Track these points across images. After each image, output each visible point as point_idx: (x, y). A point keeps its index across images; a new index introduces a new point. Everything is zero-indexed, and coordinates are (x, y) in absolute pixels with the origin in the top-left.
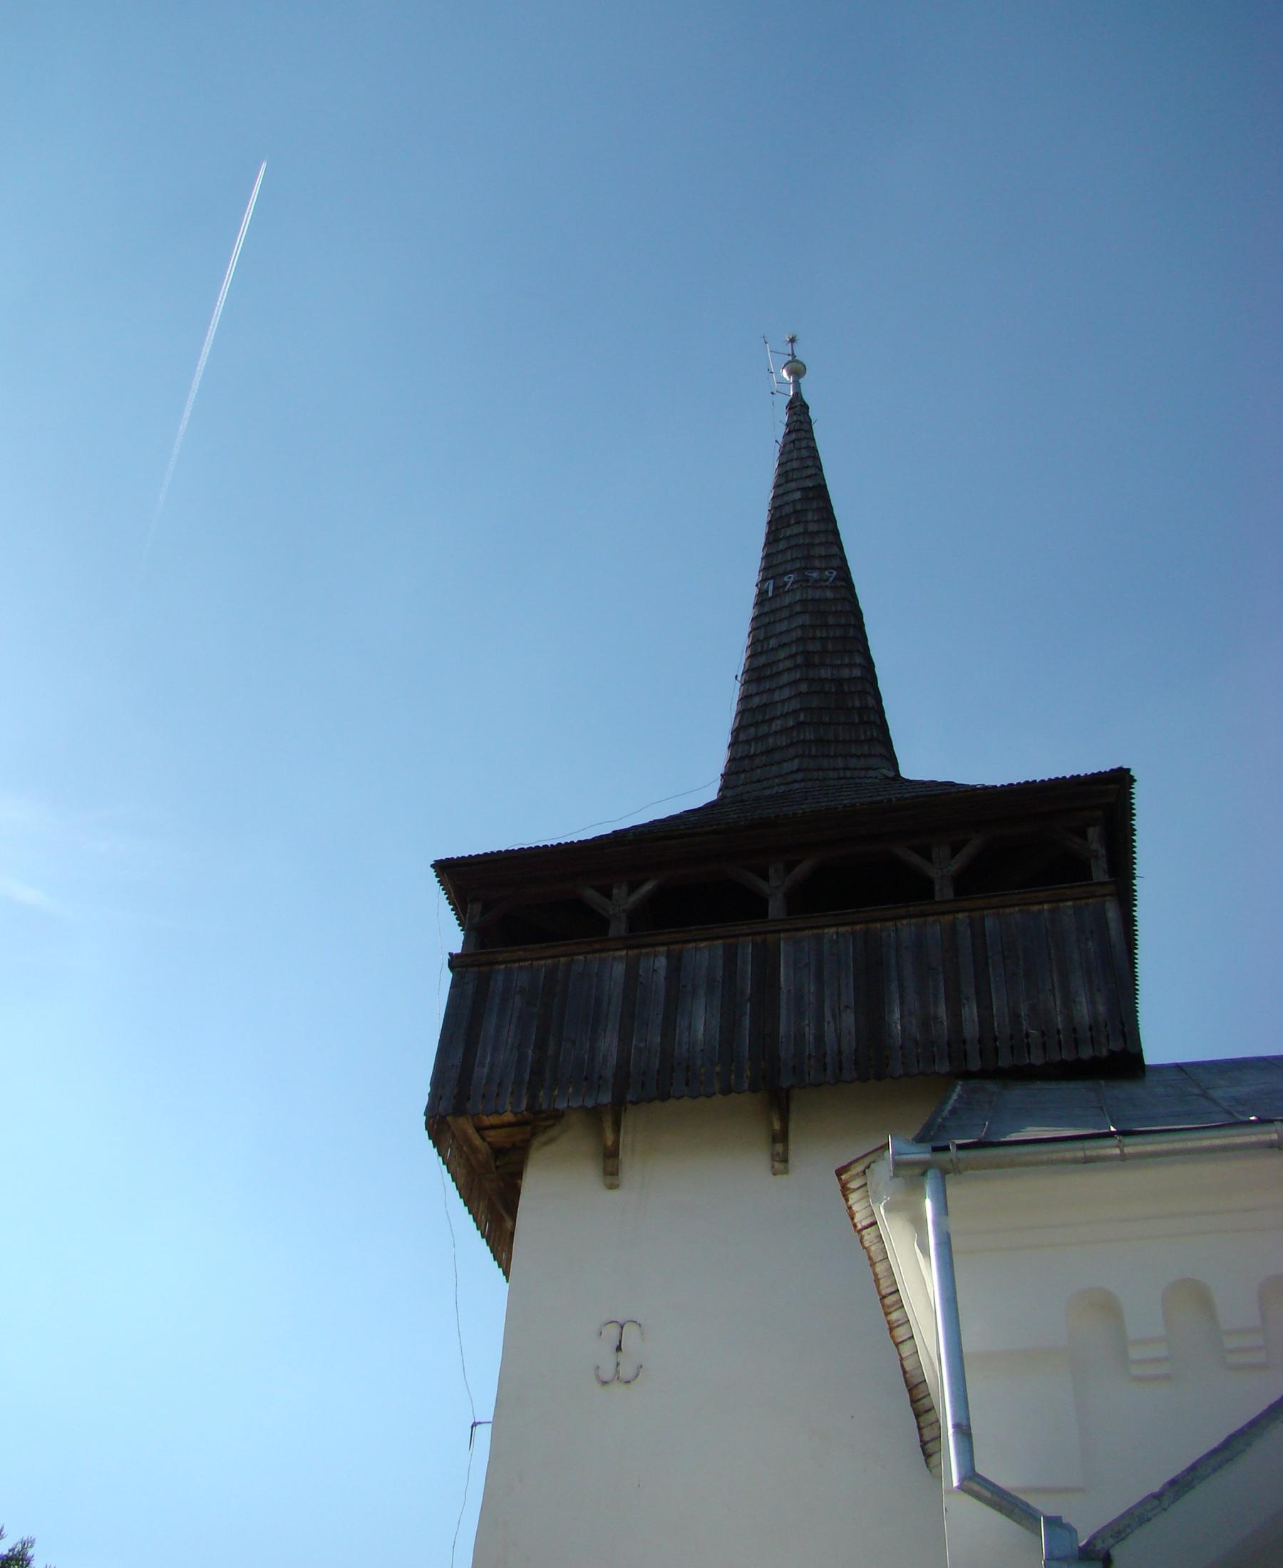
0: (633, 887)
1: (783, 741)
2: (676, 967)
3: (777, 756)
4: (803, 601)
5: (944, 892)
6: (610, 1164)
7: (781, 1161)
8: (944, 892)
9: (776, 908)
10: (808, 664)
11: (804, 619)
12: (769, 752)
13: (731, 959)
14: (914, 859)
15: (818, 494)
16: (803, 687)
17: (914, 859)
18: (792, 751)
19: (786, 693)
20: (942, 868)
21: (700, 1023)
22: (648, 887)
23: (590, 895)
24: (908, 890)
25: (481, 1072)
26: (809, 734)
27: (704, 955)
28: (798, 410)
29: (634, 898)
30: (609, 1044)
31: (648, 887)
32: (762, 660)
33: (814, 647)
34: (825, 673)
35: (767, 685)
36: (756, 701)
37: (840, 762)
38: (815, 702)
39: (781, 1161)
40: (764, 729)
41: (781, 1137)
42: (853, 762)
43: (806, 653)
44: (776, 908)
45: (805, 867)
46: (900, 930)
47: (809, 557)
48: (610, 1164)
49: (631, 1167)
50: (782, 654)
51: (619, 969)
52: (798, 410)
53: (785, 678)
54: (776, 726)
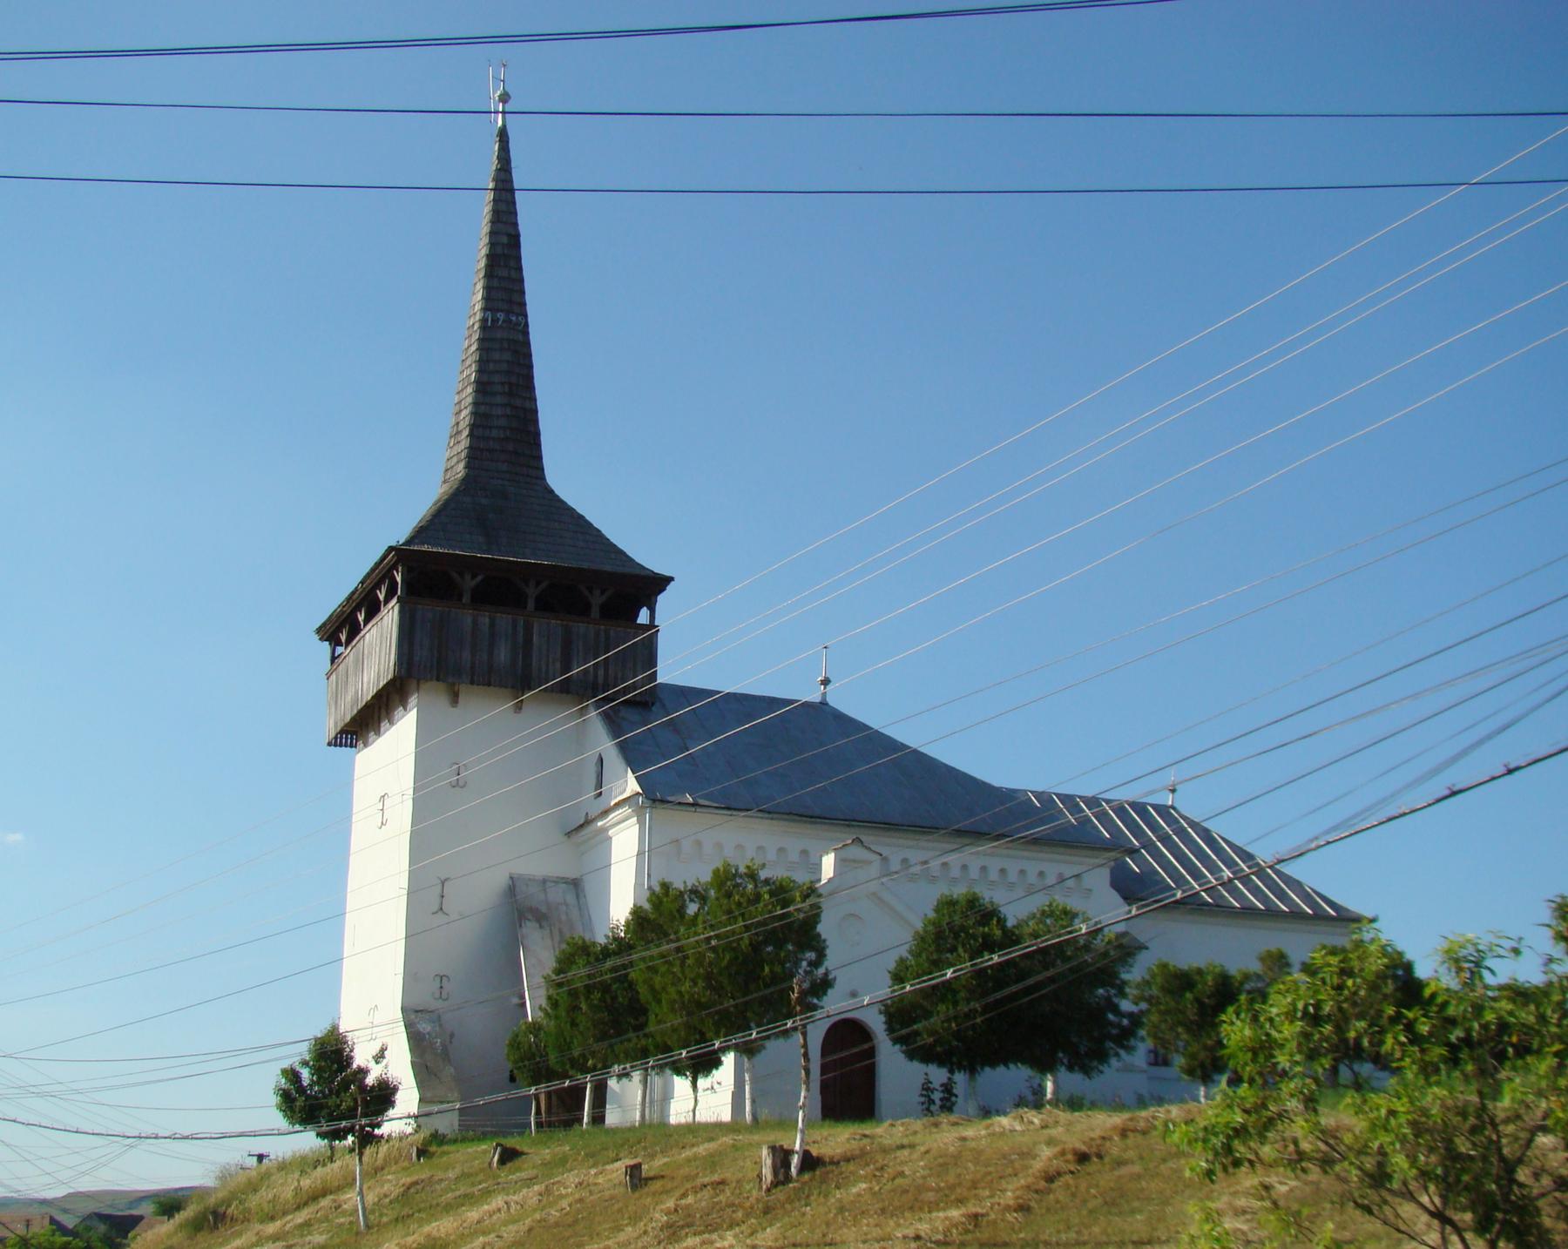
0: (474, 577)
2: (492, 625)
5: (595, 613)
6: (455, 699)
8: (595, 613)
9: (531, 604)
11: (507, 356)
13: (515, 627)
14: (586, 593)
15: (514, 241)
16: (508, 411)
17: (586, 593)
19: (499, 411)
20: (597, 600)
21: (503, 655)
22: (480, 578)
23: (455, 575)
24: (583, 610)
25: (416, 659)
26: (510, 447)
27: (504, 620)
28: (503, 135)
29: (474, 583)
30: (466, 655)
31: (480, 578)
32: (485, 378)
33: (514, 380)
36: (482, 409)
44: (531, 604)
45: (544, 585)
46: (580, 628)
47: (510, 302)
48: (455, 699)
50: (496, 378)
51: (469, 620)
52: (503, 135)
53: (499, 400)
54: (495, 433)
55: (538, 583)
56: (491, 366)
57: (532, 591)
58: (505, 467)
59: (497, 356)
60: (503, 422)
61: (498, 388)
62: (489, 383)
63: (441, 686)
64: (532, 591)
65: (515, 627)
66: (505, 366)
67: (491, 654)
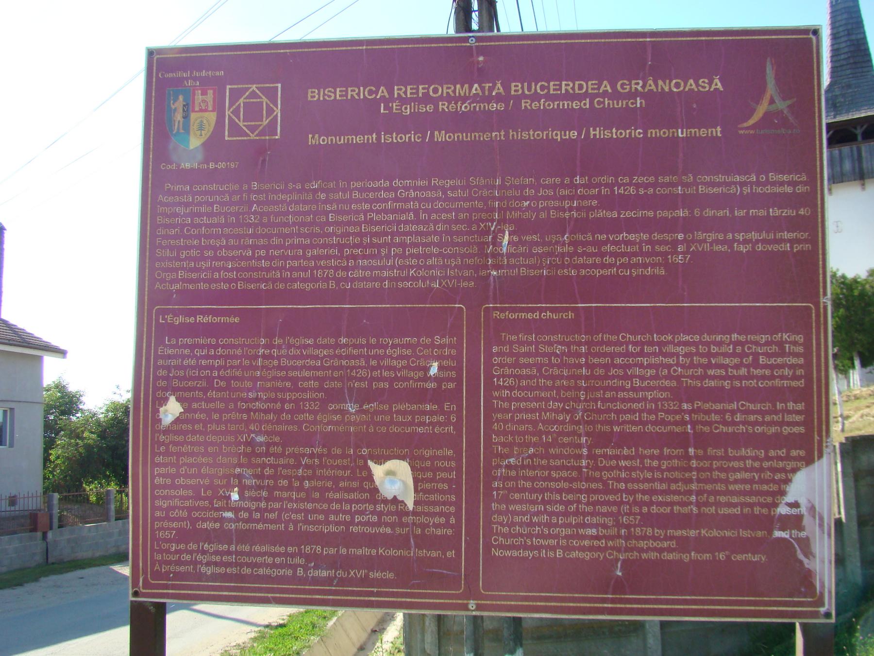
1: (845, 63)
3: (844, 68)
4: (845, 8)
7: (864, 189)
9: (859, 138)
10: (849, 35)
11: (845, 16)
12: (841, 66)
13: (852, 151)
16: (848, 43)
18: (848, 66)
19: (843, 45)
21: (847, 166)
26: (851, 61)
27: (846, 149)
33: (849, 27)
34: (853, 37)
35: (839, 41)
36: (836, 47)
37: (860, 70)
38: (852, 49)
39: (864, 189)
40: (839, 58)
41: (863, 185)
42: (865, 70)
43: (848, 30)
44: (859, 138)
45: (865, 127)
49: (833, 191)
50: (841, 29)
53: (843, 39)
54: (843, 57)
55: (862, 126)
56: (837, 24)
57: (859, 132)
58: (848, 72)
59: (839, 18)
60: (846, 50)
61: (842, 34)
62: (838, 33)
63: (857, 182)
64: (859, 132)
65: (852, 151)
66: (844, 22)
67: (841, 167)
